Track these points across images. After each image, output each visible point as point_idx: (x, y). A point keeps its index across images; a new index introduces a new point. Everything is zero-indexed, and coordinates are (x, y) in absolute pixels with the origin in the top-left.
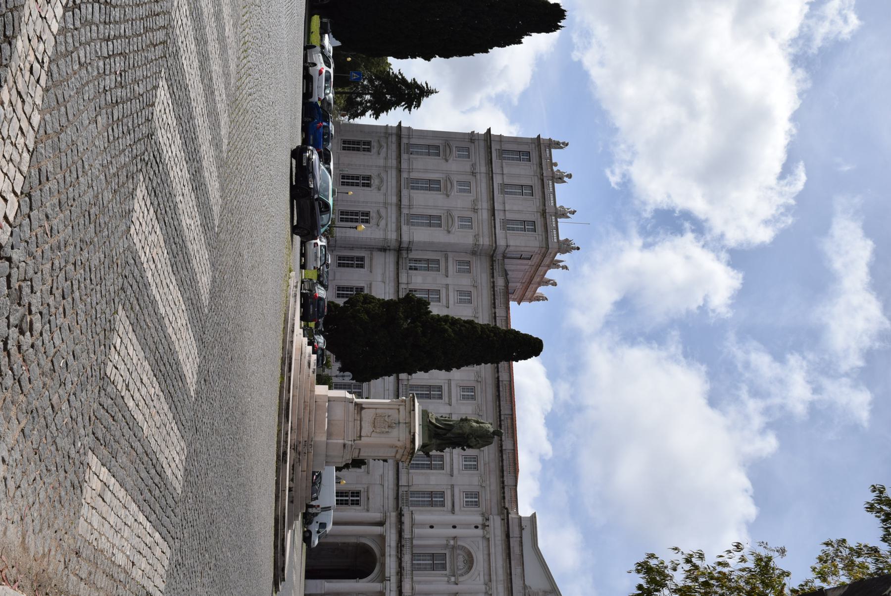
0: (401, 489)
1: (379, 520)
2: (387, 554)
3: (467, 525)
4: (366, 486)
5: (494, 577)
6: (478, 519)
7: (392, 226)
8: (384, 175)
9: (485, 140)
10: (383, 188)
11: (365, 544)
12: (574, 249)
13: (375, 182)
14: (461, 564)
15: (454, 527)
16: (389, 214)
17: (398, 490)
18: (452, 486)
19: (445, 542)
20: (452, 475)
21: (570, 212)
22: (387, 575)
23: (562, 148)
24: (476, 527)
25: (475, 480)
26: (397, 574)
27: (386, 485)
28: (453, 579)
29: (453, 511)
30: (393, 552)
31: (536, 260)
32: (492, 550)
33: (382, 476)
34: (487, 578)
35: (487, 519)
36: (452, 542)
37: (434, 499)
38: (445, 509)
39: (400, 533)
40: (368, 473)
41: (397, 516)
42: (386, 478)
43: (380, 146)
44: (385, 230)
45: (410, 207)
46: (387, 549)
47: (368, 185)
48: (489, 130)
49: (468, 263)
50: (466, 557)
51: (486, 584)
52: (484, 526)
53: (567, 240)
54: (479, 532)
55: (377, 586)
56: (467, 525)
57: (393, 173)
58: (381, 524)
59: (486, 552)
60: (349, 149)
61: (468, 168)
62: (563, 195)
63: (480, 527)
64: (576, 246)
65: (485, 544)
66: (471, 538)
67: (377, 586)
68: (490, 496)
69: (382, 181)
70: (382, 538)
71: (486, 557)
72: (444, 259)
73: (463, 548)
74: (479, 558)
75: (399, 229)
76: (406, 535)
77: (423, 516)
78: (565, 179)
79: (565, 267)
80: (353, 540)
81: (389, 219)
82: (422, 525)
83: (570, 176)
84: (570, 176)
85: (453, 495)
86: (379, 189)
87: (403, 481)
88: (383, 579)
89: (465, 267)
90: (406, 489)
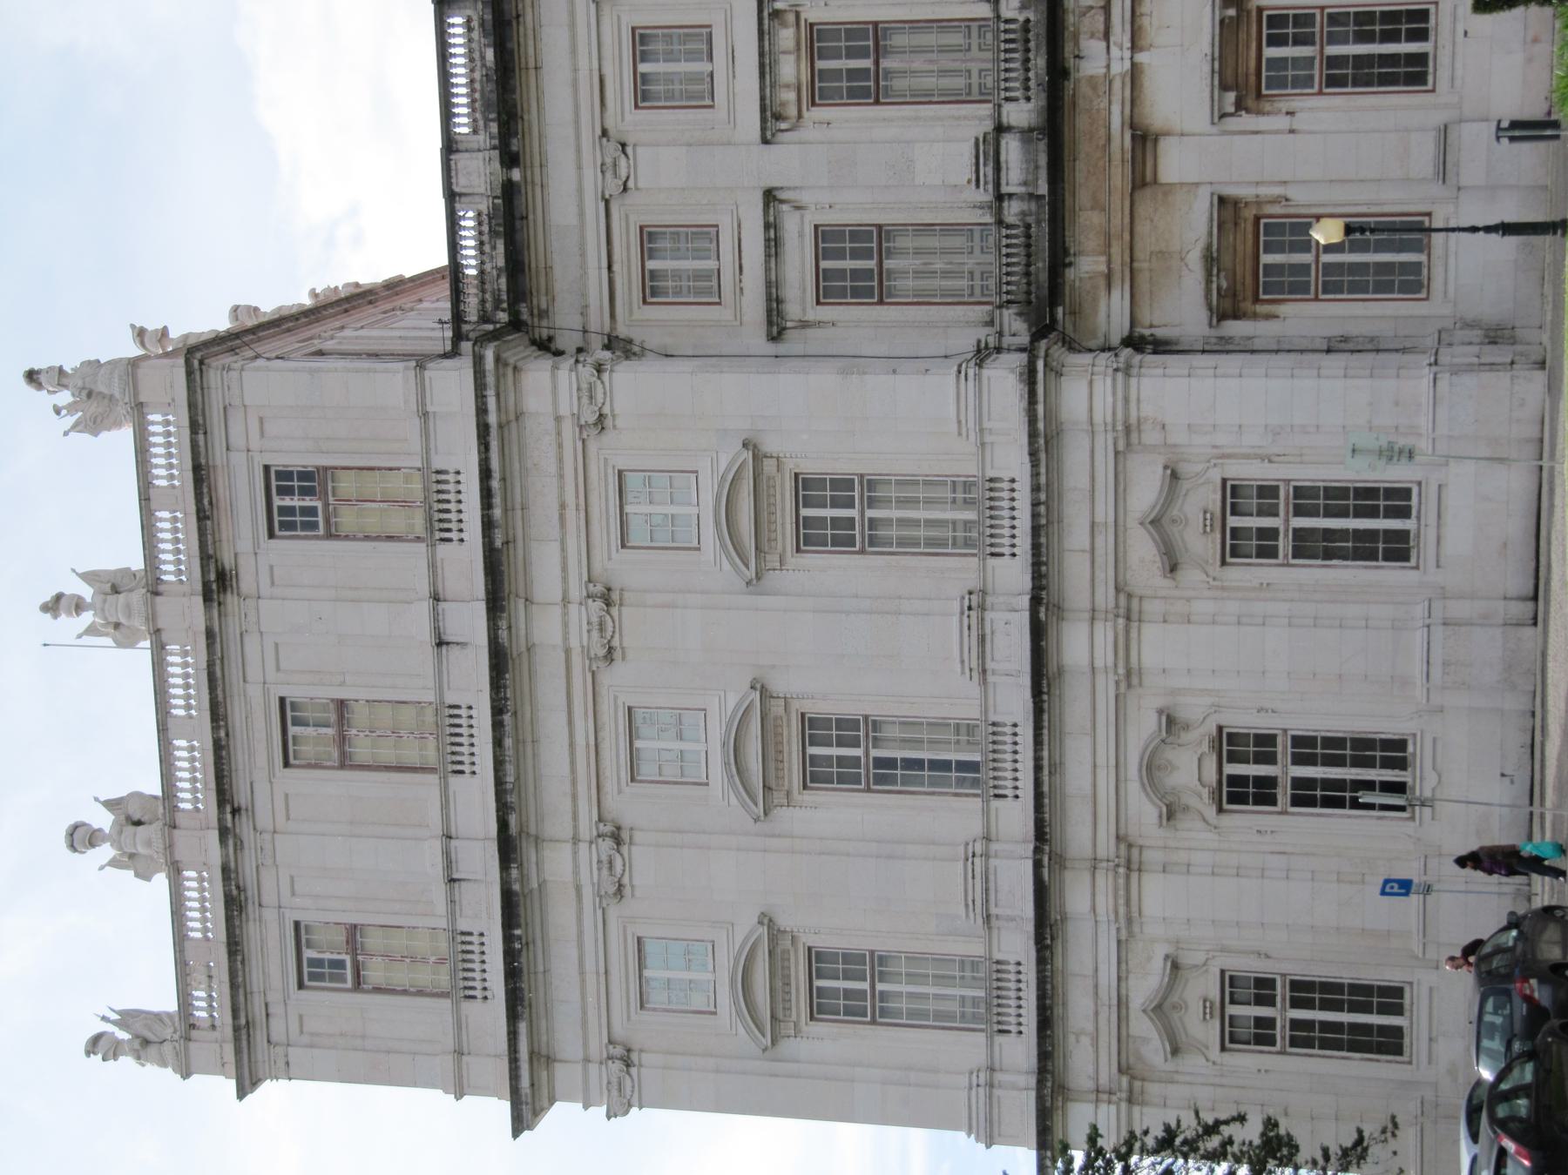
7: (1081, 463)
8: (1143, 812)
9: (543, 1058)
10: (1143, 726)
12: (60, 377)
13: (1192, 770)
16: (1105, 542)
21: (79, 606)
23: (127, 1018)
43: (1160, 1010)
44: (1128, 434)
45: (977, 603)
47: (1231, 744)
48: (520, 1124)
49: (652, 288)
53: (93, 425)
57: (1081, 833)
60: (1363, 996)
61: (643, 864)
62: (111, 721)
64: (44, 400)
69: (1152, 769)
72: (793, 310)
75: (1043, 441)
78: (104, 820)
81: (1104, 512)
83: (80, 837)
84: (80, 837)
86: (1171, 722)
89: (666, 261)
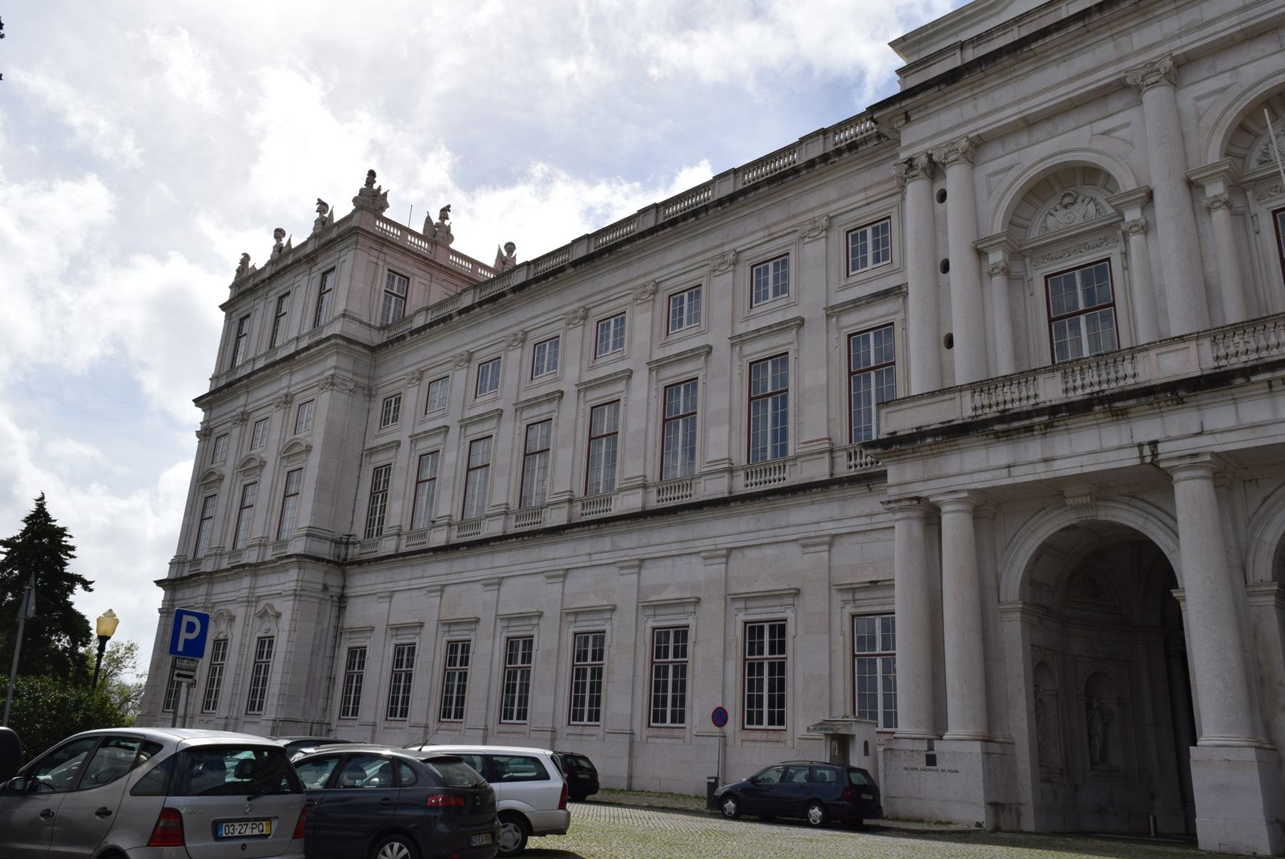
0: (843, 470)
1: (917, 528)
2: (1043, 473)
3: (936, 226)
4: (838, 598)
5: (1107, 75)
6: (917, 190)
11: (1031, 581)
14: (1079, 215)
15: (945, 267)
17: (841, 482)
18: (833, 312)
19: (998, 282)
20: (800, 323)
22: (1130, 459)
24: (942, 196)
25: (814, 250)
26: (1120, 415)
27: (831, 528)
28: (1133, 215)
29: (898, 292)
30: (1033, 449)
31: (407, 267)
32: (1010, 115)
33: (807, 544)
34: (1115, 103)
35: (910, 162)
36: (996, 257)
37: (869, 364)
38: (897, 319)
39: (954, 433)
40: (797, 593)
41: (899, 457)
42: (811, 530)
46: (1024, 475)
50: (1053, 203)
51: (1138, 89)
52: (935, 169)
54: (954, 178)
55: (1192, 497)
56: (936, 226)
58: (931, 515)
59: (1024, 139)
63: (938, 186)
65: (995, 149)
66: (979, 199)
67: (1192, 497)
68: (847, 195)
70: (989, 508)
71: (1039, 133)
73: (1014, 221)
74: (1037, 154)
76: (962, 409)
77: (915, 373)
79: (445, 212)
80: (1012, 631)
82: (943, 369)
85: (856, 304)
87: (818, 470)
88: (1151, 480)
90: (842, 459)
